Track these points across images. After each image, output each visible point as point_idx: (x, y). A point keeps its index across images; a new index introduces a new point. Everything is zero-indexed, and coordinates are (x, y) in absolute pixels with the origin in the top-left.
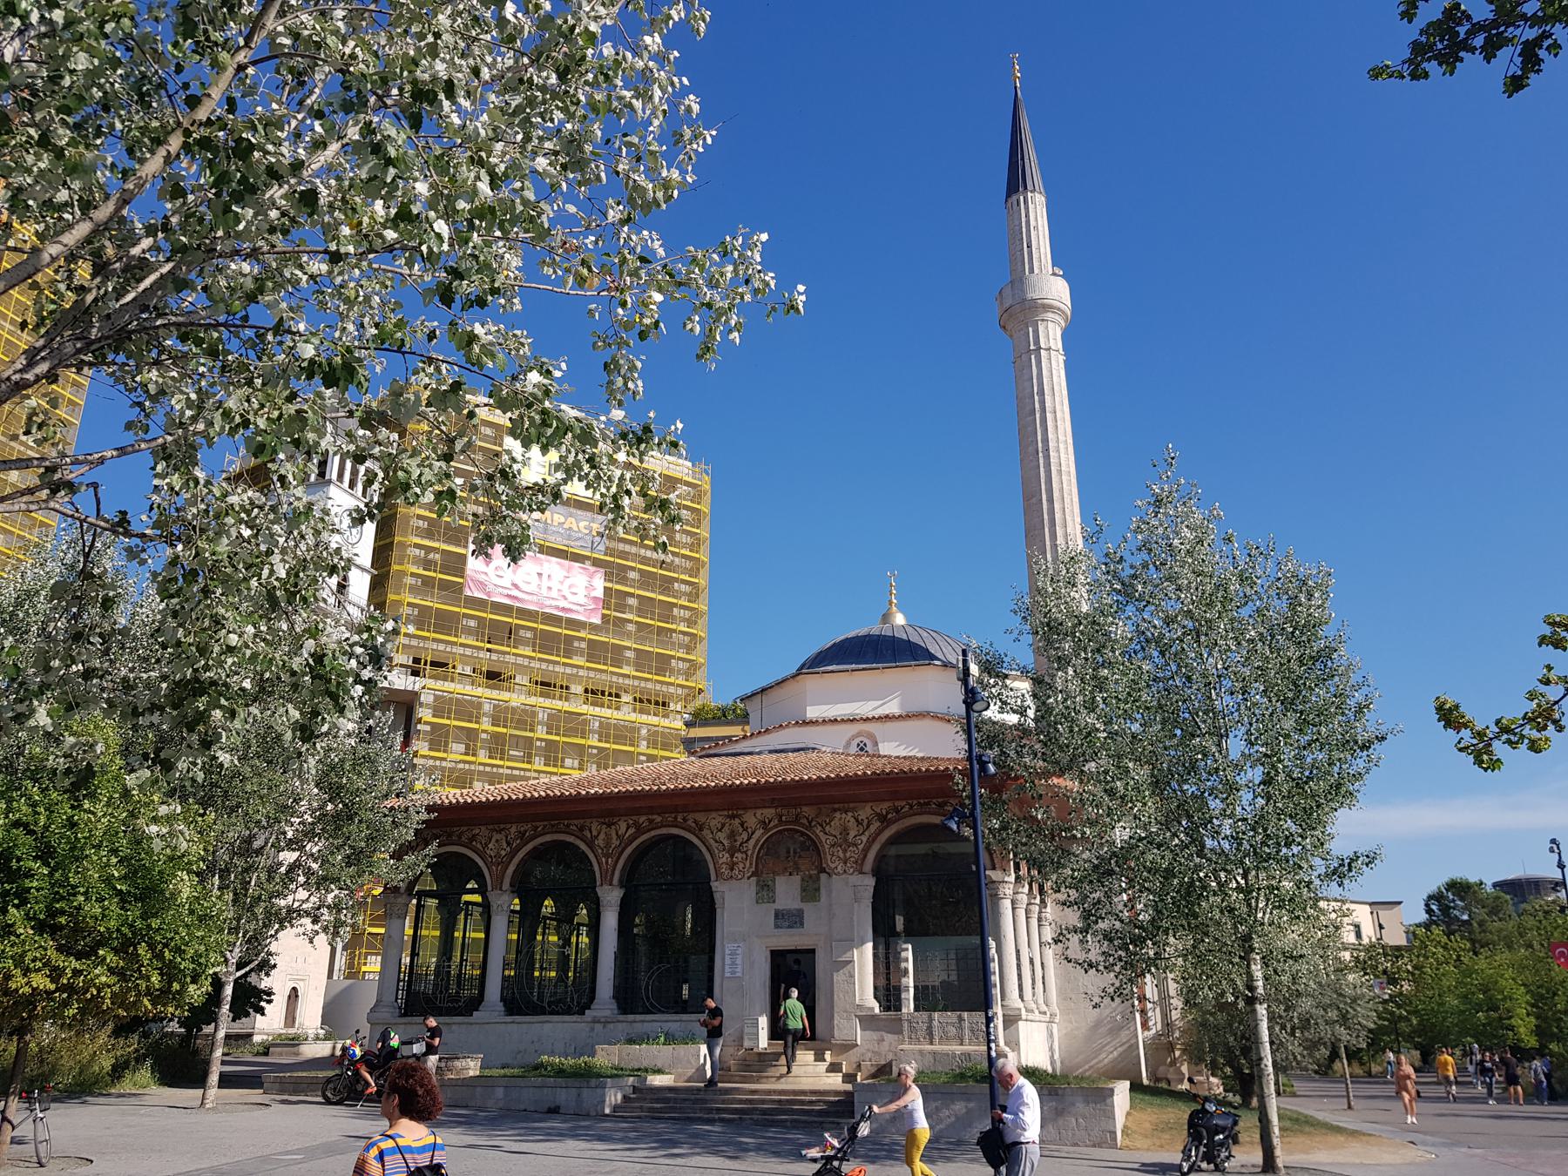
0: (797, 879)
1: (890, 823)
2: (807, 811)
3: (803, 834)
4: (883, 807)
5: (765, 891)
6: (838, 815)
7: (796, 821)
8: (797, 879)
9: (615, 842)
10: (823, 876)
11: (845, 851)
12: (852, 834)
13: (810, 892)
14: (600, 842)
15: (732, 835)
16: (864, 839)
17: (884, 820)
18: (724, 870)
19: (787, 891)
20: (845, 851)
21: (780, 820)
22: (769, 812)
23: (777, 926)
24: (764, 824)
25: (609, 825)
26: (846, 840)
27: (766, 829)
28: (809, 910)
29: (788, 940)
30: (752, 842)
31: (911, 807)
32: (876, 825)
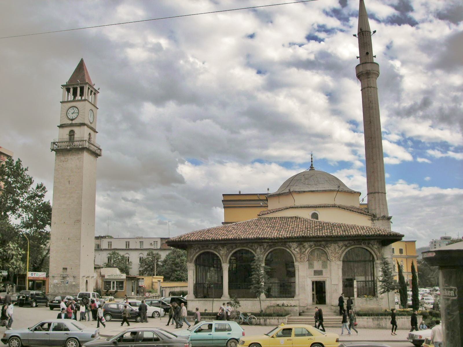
0: (320, 262)
1: (348, 247)
2: (323, 243)
3: (322, 250)
4: (346, 243)
5: (311, 265)
6: (332, 244)
7: (320, 246)
8: (320, 262)
9: (263, 251)
10: (328, 262)
11: (335, 255)
12: (337, 250)
13: (325, 266)
14: (258, 250)
16: (341, 251)
17: (346, 246)
18: (299, 259)
19: (317, 266)
20: (335, 255)
21: (315, 245)
22: (312, 243)
23: (314, 275)
24: (311, 246)
25: (260, 246)
26: (335, 251)
27: (311, 248)
28: (324, 271)
30: (307, 252)
31: (354, 243)
32: (344, 248)
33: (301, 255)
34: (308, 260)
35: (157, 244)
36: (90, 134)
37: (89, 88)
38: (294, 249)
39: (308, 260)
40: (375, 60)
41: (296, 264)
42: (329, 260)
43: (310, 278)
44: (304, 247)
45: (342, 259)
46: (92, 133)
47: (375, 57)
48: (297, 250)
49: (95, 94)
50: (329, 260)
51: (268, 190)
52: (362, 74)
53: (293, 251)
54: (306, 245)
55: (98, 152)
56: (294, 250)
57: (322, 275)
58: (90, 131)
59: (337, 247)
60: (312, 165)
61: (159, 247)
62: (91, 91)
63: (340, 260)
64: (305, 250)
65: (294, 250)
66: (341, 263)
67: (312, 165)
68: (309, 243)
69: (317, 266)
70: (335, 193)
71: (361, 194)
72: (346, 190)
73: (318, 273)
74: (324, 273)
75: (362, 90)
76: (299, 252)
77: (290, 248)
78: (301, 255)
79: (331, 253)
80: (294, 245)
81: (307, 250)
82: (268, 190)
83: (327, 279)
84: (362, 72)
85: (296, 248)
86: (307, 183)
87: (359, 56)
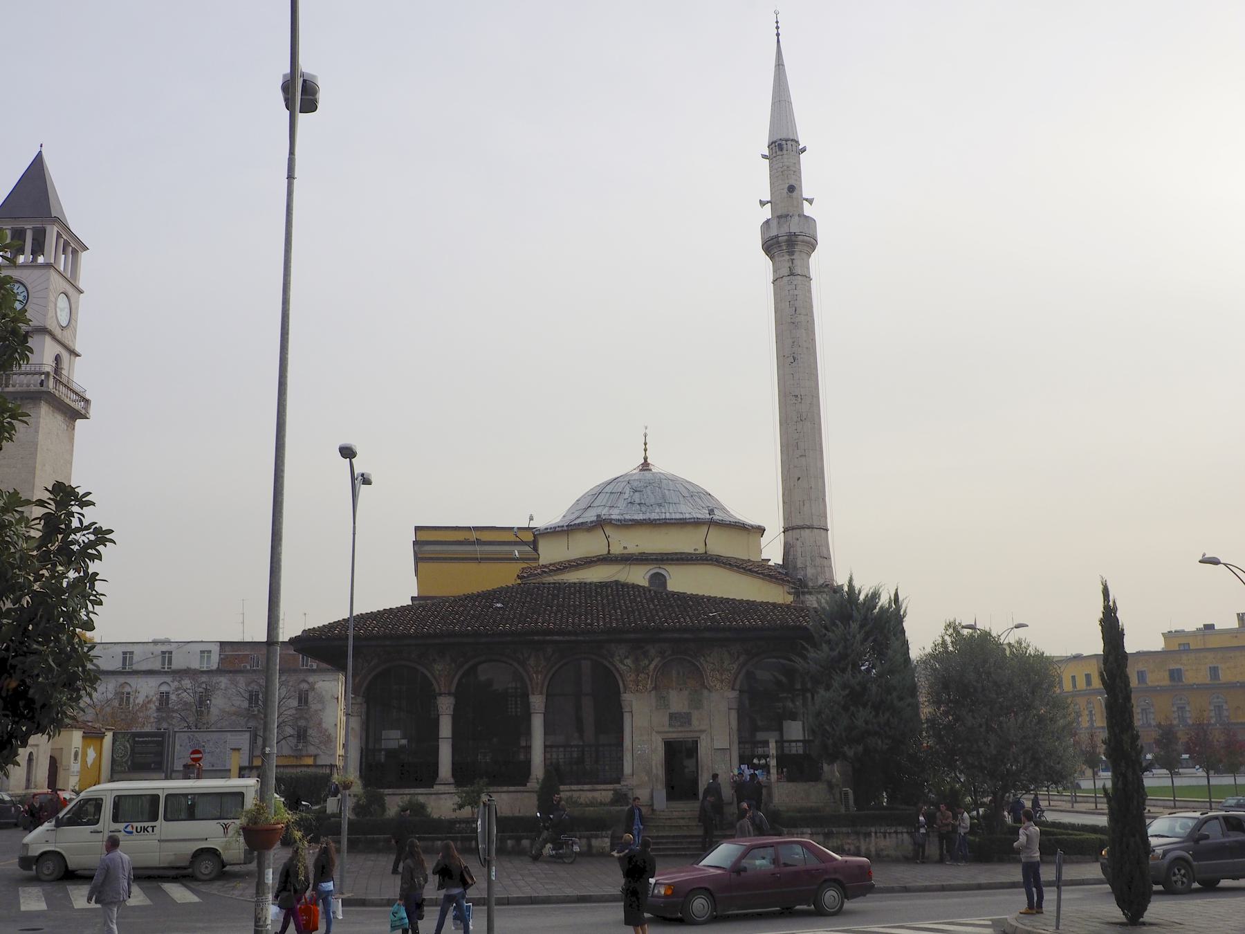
5: (663, 702)
10: (706, 692)
13: (696, 703)
14: (532, 662)
15: (636, 660)
19: (678, 701)
30: (652, 666)
32: (741, 659)
34: (655, 688)
35: (209, 657)
36: (58, 358)
37: (59, 235)
39: (655, 688)
40: (808, 210)
41: (626, 697)
43: (658, 732)
45: (737, 687)
46: (65, 355)
47: (810, 201)
48: (628, 661)
49: (75, 252)
51: (531, 519)
52: (778, 242)
55: (79, 406)
57: (690, 724)
58: (59, 349)
60: (646, 459)
61: (215, 667)
62: (66, 244)
63: (733, 689)
65: (621, 662)
66: (735, 694)
67: (646, 459)
70: (705, 529)
72: (727, 519)
74: (695, 722)
75: (774, 282)
79: (713, 670)
81: (654, 663)
82: (531, 519)
83: (703, 736)
84: (777, 237)
85: (627, 657)
86: (637, 501)
87: (767, 197)
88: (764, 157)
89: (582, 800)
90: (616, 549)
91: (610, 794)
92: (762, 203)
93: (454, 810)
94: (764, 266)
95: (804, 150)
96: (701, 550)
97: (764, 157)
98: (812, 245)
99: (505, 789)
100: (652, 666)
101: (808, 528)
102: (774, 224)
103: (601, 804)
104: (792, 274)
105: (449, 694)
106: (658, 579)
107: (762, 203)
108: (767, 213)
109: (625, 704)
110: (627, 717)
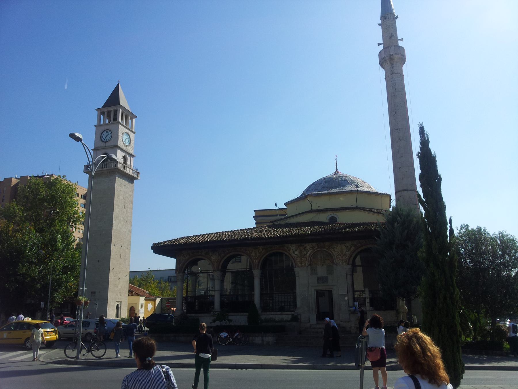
6: (339, 245)
11: (342, 257)
12: (344, 251)
14: (253, 254)
15: (301, 252)
16: (349, 253)
20: (342, 257)
23: (318, 283)
24: (313, 248)
29: (321, 287)
30: (308, 254)
32: (353, 248)
33: (301, 259)
34: (310, 265)
38: (294, 251)
39: (310, 265)
40: (400, 44)
41: (296, 269)
42: (334, 264)
44: (305, 248)
45: (351, 263)
47: (402, 40)
48: (297, 252)
50: (334, 264)
53: (293, 255)
54: (308, 246)
56: (294, 253)
59: (344, 248)
60: (337, 169)
63: (348, 264)
64: (305, 252)
65: (294, 253)
67: (337, 169)
68: (310, 244)
69: (321, 271)
71: (390, 196)
73: (322, 280)
76: (299, 254)
77: (289, 251)
78: (301, 259)
80: (293, 247)
84: (385, 58)
85: (296, 250)
86: (326, 186)
87: (381, 42)
88: (379, 25)
89: (277, 319)
90: (315, 207)
91: (290, 316)
92: (379, 45)
93: (211, 323)
94: (381, 73)
95: (397, 17)
96: (355, 206)
97: (379, 25)
98: (403, 60)
99: (242, 314)
100: (308, 254)
101: (406, 190)
102: (383, 52)
103: (286, 321)
104: (393, 73)
105: (218, 270)
106: (333, 220)
107: (379, 45)
108: (381, 47)
109: (296, 273)
110: (297, 278)
